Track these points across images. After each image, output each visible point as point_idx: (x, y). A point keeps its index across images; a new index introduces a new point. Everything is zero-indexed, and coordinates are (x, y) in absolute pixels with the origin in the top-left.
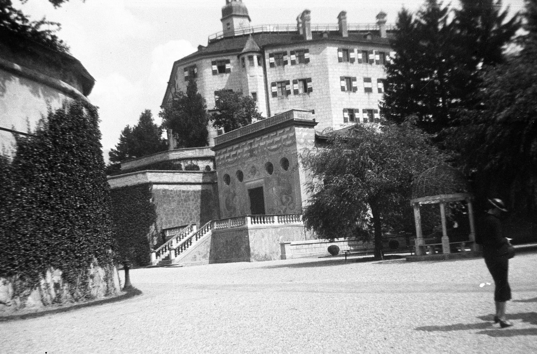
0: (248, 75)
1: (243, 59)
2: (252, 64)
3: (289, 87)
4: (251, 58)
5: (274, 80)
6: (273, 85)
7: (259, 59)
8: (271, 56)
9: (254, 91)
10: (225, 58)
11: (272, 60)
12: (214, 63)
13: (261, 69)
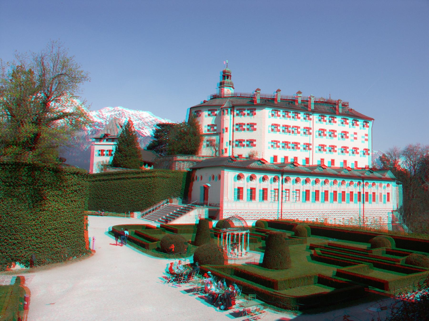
0: (224, 119)
1: (223, 111)
2: (228, 113)
3: (244, 127)
4: (227, 110)
5: (238, 122)
6: (237, 124)
7: (231, 110)
8: (237, 110)
9: (226, 127)
10: (216, 108)
11: (238, 112)
12: (209, 110)
13: (232, 116)
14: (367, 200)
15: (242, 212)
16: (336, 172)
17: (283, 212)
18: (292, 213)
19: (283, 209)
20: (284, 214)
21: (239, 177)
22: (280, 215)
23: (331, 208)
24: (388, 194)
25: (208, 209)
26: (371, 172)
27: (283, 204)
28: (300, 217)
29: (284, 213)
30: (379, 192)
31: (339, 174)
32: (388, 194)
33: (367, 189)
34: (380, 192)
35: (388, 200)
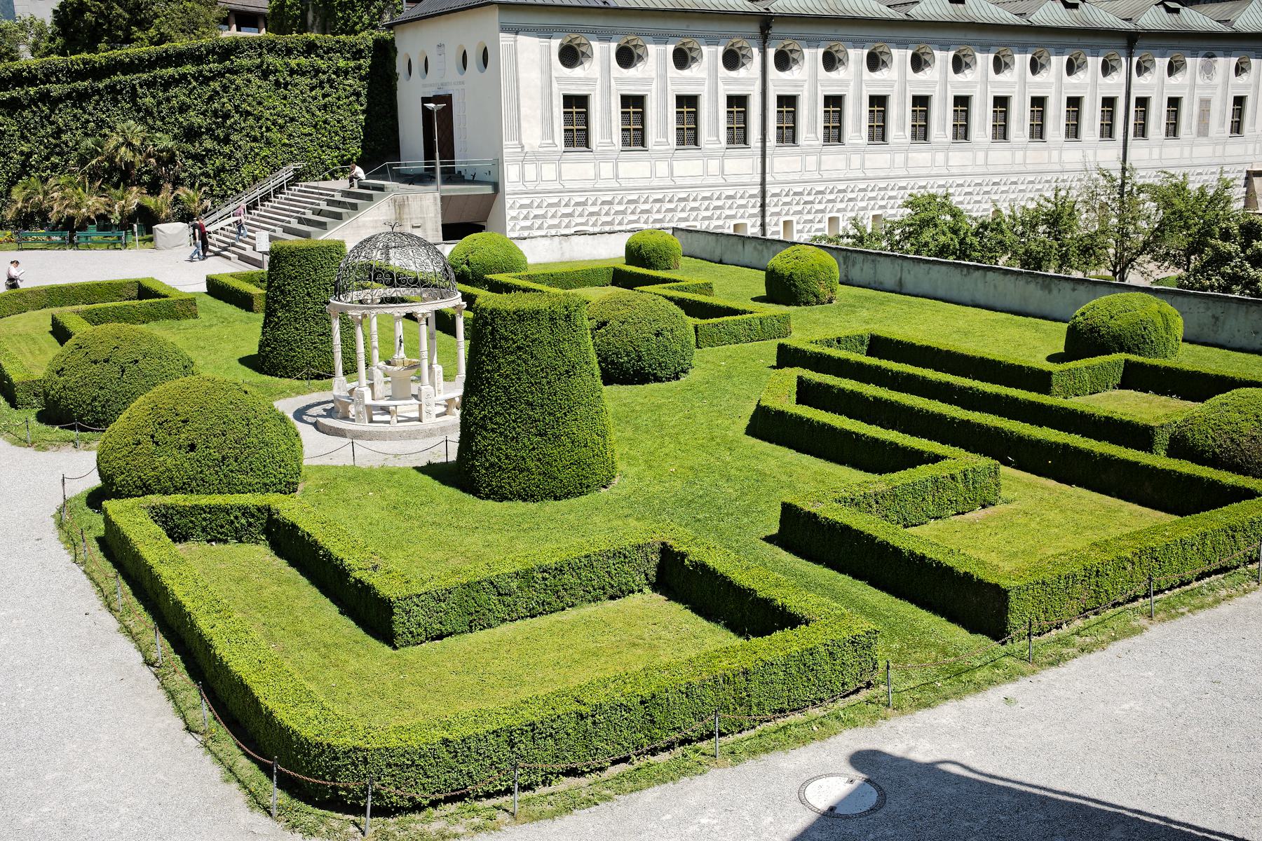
14: (1142, 131)
15: (590, 202)
16: (1009, 15)
17: (768, 194)
18: (809, 194)
19: (768, 178)
20: (775, 199)
21: (570, 56)
22: (759, 204)
23: (983, 170)
24: (1239, 101)
25: (438, 195)
26: (1169, 10)
27: (767, 160)
28: (844, 210)
29: (774, 195)
30: (1199, 94)
31: (1023, 22)
32: (1239, 101)
33: (1144, 85)
34: (1206, 94)
35: (1237, 128)
